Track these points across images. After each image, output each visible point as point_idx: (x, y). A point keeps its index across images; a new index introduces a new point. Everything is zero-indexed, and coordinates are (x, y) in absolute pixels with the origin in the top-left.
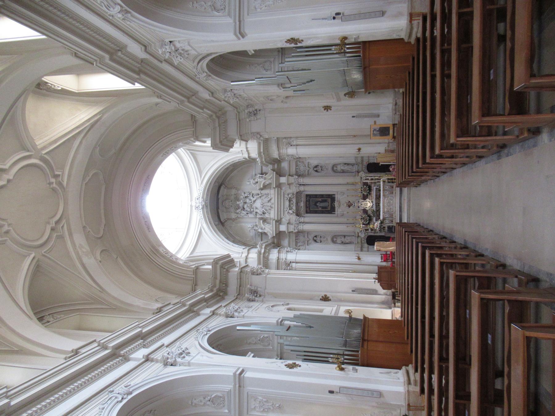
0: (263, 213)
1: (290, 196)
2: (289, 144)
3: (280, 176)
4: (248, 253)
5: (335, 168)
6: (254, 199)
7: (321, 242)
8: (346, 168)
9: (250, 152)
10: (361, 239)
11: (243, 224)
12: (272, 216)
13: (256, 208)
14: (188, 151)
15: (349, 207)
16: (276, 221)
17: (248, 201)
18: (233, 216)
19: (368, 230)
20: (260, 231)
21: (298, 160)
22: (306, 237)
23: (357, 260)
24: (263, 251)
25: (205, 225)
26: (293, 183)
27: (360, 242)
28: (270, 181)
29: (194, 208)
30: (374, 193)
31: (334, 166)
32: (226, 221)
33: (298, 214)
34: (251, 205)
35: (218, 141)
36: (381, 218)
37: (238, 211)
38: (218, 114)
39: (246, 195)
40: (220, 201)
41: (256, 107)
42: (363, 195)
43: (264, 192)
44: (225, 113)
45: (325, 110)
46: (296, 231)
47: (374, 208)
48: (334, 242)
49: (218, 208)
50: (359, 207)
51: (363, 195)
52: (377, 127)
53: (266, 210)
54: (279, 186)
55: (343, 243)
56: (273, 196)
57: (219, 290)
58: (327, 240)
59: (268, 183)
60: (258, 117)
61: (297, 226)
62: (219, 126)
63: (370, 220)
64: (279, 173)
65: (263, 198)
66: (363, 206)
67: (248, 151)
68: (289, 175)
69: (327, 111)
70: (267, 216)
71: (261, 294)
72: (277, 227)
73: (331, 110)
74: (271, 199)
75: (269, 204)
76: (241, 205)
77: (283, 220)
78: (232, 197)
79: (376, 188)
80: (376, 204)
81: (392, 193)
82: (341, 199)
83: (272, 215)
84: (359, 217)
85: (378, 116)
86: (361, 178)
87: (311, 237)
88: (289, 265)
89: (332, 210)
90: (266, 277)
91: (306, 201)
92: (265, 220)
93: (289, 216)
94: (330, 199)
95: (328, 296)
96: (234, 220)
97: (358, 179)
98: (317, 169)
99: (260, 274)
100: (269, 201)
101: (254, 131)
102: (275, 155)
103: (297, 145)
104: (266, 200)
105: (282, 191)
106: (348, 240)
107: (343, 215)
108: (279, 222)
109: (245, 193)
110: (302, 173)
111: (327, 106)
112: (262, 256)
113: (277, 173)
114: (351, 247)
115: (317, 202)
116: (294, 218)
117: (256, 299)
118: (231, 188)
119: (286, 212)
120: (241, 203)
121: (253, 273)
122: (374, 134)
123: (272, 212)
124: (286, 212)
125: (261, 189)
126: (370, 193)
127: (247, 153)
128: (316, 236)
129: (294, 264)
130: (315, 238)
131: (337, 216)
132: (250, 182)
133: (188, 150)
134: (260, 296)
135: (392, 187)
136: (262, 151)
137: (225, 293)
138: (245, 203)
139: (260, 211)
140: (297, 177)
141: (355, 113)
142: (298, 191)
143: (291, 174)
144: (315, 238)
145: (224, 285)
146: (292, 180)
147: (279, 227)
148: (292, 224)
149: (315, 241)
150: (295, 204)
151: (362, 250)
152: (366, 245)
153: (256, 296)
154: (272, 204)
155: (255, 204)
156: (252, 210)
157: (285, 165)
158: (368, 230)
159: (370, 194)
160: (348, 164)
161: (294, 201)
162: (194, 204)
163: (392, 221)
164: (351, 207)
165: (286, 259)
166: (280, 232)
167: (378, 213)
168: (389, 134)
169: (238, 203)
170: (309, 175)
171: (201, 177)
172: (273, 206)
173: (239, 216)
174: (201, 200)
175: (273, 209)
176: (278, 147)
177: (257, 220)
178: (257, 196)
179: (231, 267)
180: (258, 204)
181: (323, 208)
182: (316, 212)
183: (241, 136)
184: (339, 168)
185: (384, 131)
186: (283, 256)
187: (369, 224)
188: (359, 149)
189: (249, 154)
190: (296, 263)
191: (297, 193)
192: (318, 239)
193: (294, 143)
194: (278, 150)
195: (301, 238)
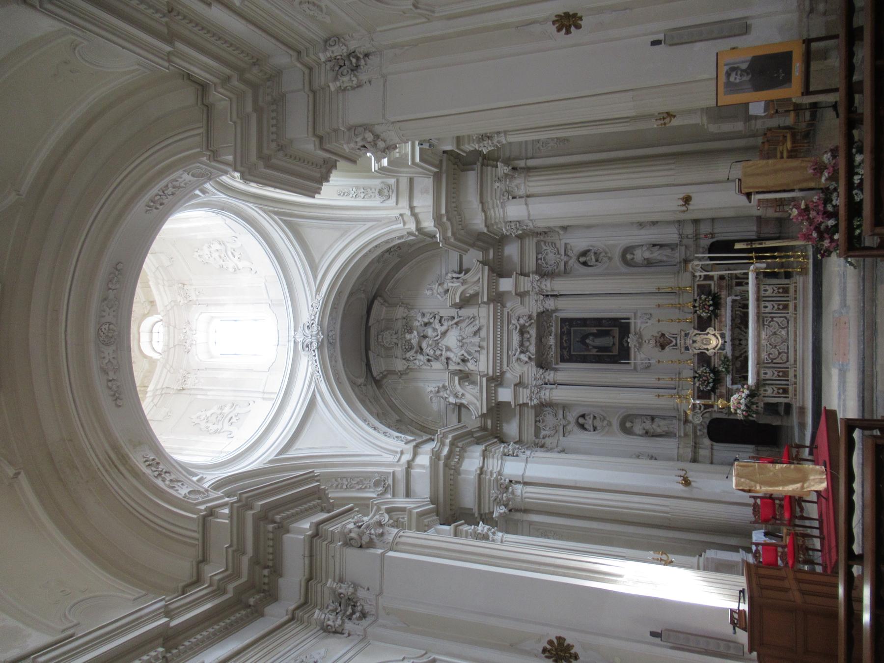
0: (464, 361)
1: (522, 321)
2: (508, 192)
3: (501, 275)
4: (415, 454)
5: (629, 257)
6: (444, 328)
7: (595, 429)
8: (656, 254)
9: (421, 216)
10: (695, 428)
11: (421, 384)
12: (482, 367)
13: (448, 349)
14: (276, 217)
15: (663, 347)
16: (490, 380)
17: (429, 332)
18: (400, 365)
20: (452, 400)
21: (541, 235)
22: (561, 417)
23: (681, 487)
24: (445, 451)
25: (323, 387)
26: (528, 292)
27: (691, 433)
28: (476, 288)
29: (300, 347)
30: (727, 313)
31: (628, 250)
32: (385, 377)
33: (542, 364)
34: (437, 343)
35: (253, 157)
36: (751, 380)
37: (409, 355)
38: (248, 76)
39: (426, 320)
40: (373, 332)
41: (353, 45)
43: (464, 312)
44: (276, 76)
45: (559, 30)
46: (535, 402)
47: (728, 350)
48: (627, 431)
49: (367, 348)
50: (687, 349)
51: (699, 317)
52: (743, 59)
53: (469, 353)
54: (497, 299)
55: (647, 434)
56: (484, 322)
57: (251, 587)
58: (610, 424)
59: (471, 292)
60: (364, 77)
61: (536, 390)
62: (258, 110)
63: (718, 380)
64: (498, 270)
65: (463, 325)
66: (697, 345)
67: (414, 215)
68: (521, 274)
69: (568, 32)
70: (471, 366)
71: (367, 608)
72: (491, 394)
73: (578, 27)
74: (479, 329)
75: (476, 340)
76: (414, 342)
77: (508, 375)
78: (399, 324)
79: (734, 301)
80: (732, 340)
81: (786, 307)
82: (645, 328)
83: (483, 365)
84: (688, 373)
85: (744, 28)
87: (572, 416)
88: (507, 488)
90: (383, 555)
91: (562, 333)
92: (465, 377)
93: (520, 368)
94: (617, 329)
95: (569, 641)
96: (401, 374)
97: (685, 280)
98: (586, 259)
99: (371, 544)
100: (475, 333)
101: (353, 120)
102: (478, 222)
103: (528, 196)
104: (472, 329)
105: (506, 311)
106: (660, 426)
107: (648, 367)
108: (496, 380)
109: (423, 315)
110: (550, 268)
111: (567, 15)
112: (441, 463)
113: (492, 270)
114: (669, 445)
115: (587, 336)
116: (531, 372)
117: (349, 626)
118: (395, 305)
119: (514, 359)
120: (414, 337)
121: (348, 542)
122: (728, 84)
123: (483, 358)
124: (514, 359)
125: (460, 306)
127: (412, 219)
128: (583, 416)
129: (519, 487)
130: (581, 421)
132: (432, 289)
133: (276, 213)
134: (364, 615)
135: (786, 291)
136: (443, 212)
137: (271, 595)
138: (425, 337)
139: (455, 356)
140: (537, 277)
141: (658, 28)
142: (542, 309)
143: (526, 270)
144: (581, 421)
145: (266, 572)
146: (526, 284)
147: (496, 393)
148: (526, 387)
149: (582, 427)
150: (533, 340)
151: (694, 460)
152: (707, 442)
153: (350, 618)
154: (482, 340)
155: (446, 339)
157: (512, 250)
159: (716, 316)
160: (661, 246)
161: (533, 332)
162: (300, 339)
163: (785, 391)
165: (500, 473)
166: (500, 404)
167: (738, 364)
168: (787, 80)
169: (408, 336)
170: (566, 272)
171: (315, 277)
172: (484, 344)
173: (411, 365)
174: (315, 329)
175: (484, 352)
176: (482, 203)
177: (446, 375)
178: (450, 323)
179: (293, 515)
180: (451, 340)
182: (584, 359)
183: (321, 138)
184: (639, 255)
185: (768, 69)
186: (493, 465)
187: (713, 390)
188: (687, 200)
189: (418, 222)
190: (526, 484)
191: (540, 315)
192: (589, 422)
193: (522, 192)
194: (484, 211)
195: (550, 420)
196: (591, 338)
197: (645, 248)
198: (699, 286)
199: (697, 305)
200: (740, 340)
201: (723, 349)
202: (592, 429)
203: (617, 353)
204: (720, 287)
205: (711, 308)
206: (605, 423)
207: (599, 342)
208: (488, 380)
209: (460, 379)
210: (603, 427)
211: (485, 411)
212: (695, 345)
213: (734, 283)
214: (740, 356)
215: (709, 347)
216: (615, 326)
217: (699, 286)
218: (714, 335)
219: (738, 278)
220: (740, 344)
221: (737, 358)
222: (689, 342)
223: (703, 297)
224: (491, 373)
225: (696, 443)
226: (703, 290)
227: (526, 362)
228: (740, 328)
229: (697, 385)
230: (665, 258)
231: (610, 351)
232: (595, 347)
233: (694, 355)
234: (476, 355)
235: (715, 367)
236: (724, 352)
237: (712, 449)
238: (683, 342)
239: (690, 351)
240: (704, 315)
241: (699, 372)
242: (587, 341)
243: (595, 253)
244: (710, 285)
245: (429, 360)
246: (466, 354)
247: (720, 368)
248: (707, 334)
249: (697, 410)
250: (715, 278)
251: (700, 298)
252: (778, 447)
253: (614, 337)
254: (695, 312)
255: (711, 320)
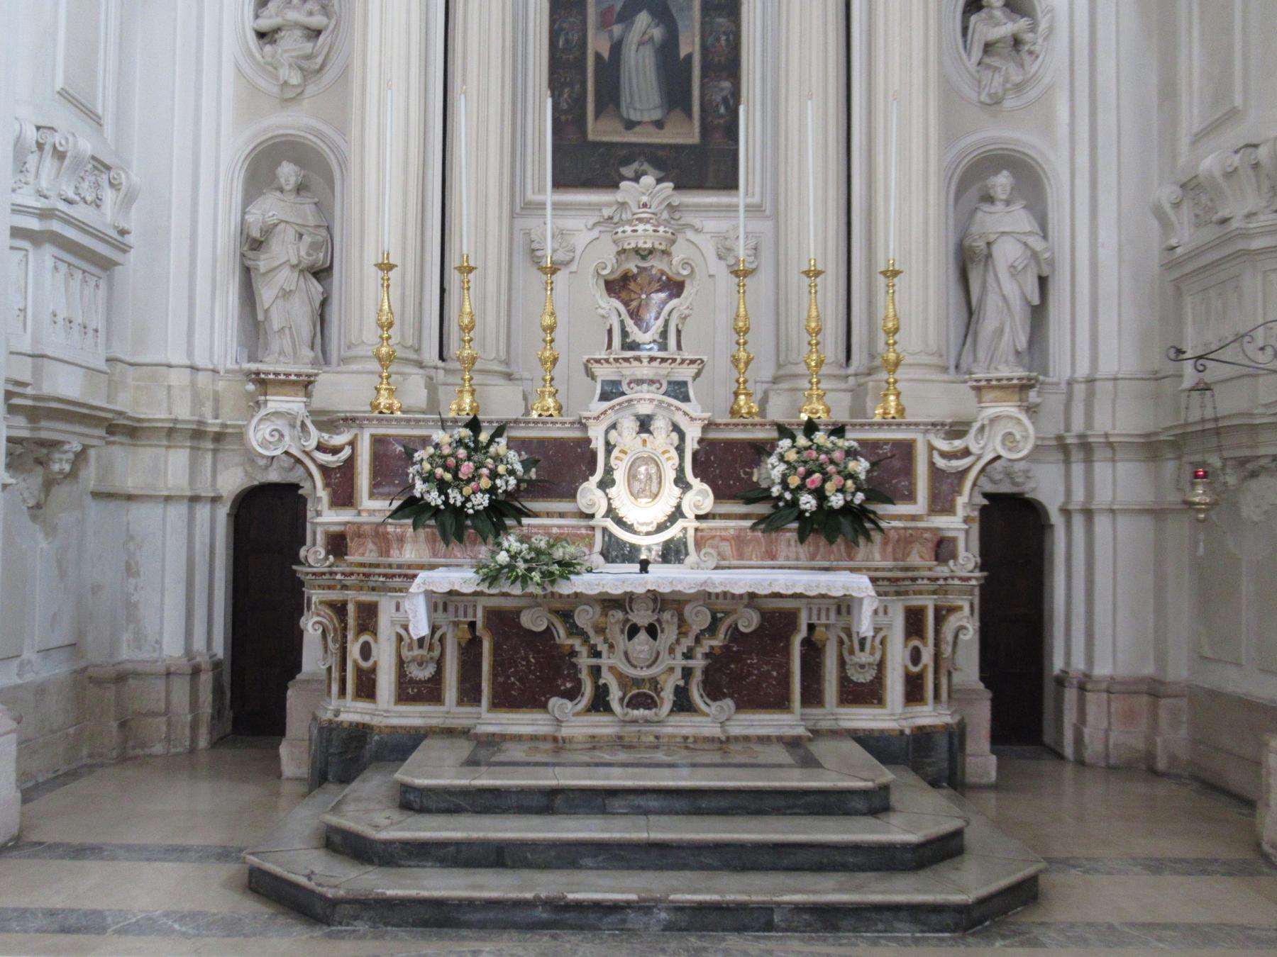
5: (1002, 182)
8: (1006, 292)
15: (618, 286)
19: (344, 496)
42: (761, 450)
48: (261, 169)
50: (611, 392)
51: (761, 450)
55: (254, 244)
58: (289, 97)
63: (453, 525)
66: (627, 436)
79: (845, 606)
80: (658, 601)
84: (502, 402)
86: (956, 430)
89: (583, 163)
94: (694, 138)
106: (287, 306)
107: (533, 255)
126: (778, 515)
131: (520, 208)
152: (232, 481)
158: (344, 496)
159: (769, 524)
160: (1038, 314)
164: (611, 306)
181: (610, 70)
184: (1006, 225)
187: (413, 508)
196: (657, 33)
197: (1037, 243)
198: (906, 450)
199: (820, 437)
200: (652, 631)
201: (606, 555)
202: (265, 23)
203: (591, 137)
204: (906, 540)
205: (808, 502)
206: (295, 79)
207: (640, 72)
210: (271, 68)
212: (629, 425)
213: (916, 601)
214: (574, 630)
215: (619, 492)
216: (705, 130)
217: (906, 450)
218: (677, 514)
219: (939, 619)
220: (633, 631)
221: (566, 616)
222: (646, 401)
223: (860, 466)
225: (219, 437)
226: (890, 470)
228: (712, 629)
229: (439, 436)
230: (989, 324)
231: (597, 117)
232: (616, 48)
233: (584, 427)
235: (520, 513)
236: (598, 559)
237: (194, 499)
238: (644, 371)
239: (598, 407)
240: (774, 469)
241: (501, 446)
242: (643, 19)
243: (1017, 42)
244: (910, 497)
247: (511, 542)
248: (680, 481)
249: (315, 436)
250: (940, 521)
251: (851, 453)
252: (215, 744)
253: (659, 124)
254: (784, 431)
255: (749, 501)
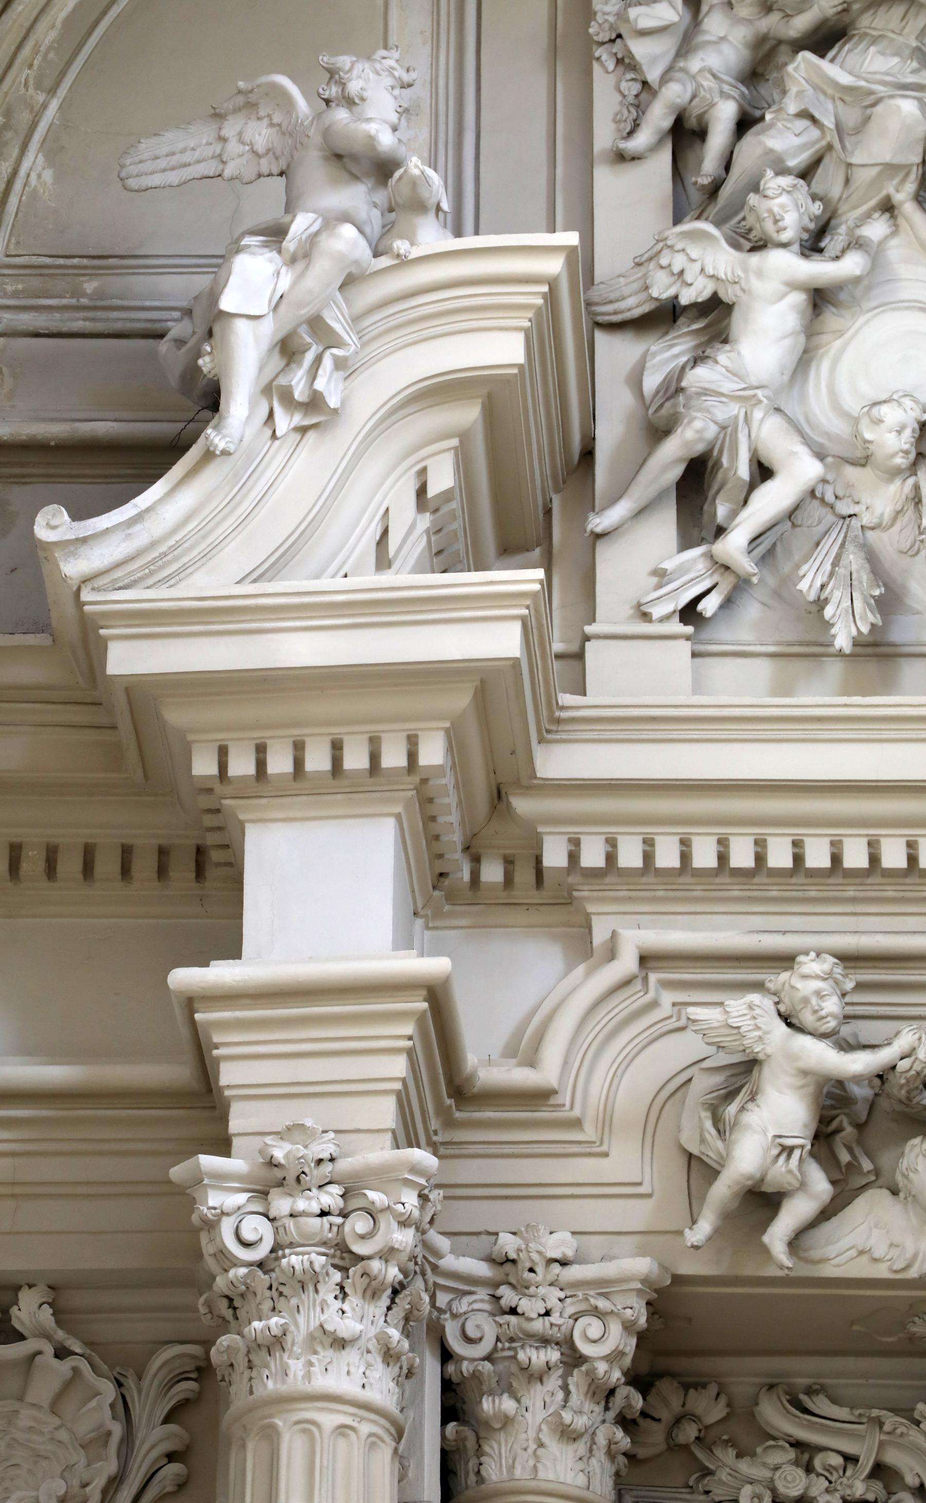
0: (697, 480)
70: (642, 558)
72: (325, 739)
92: (527, 488)
116: (599, 1238)
147: (341, 787)
156: (785, 206)
166: (198, 878)
208: (486, 683)
209: (491, 392)
211: (125, 659)
224: (557, 762)
227: (700, 1169)
234: (750, 624)
245: (685, 134)
246: (770, 501)
